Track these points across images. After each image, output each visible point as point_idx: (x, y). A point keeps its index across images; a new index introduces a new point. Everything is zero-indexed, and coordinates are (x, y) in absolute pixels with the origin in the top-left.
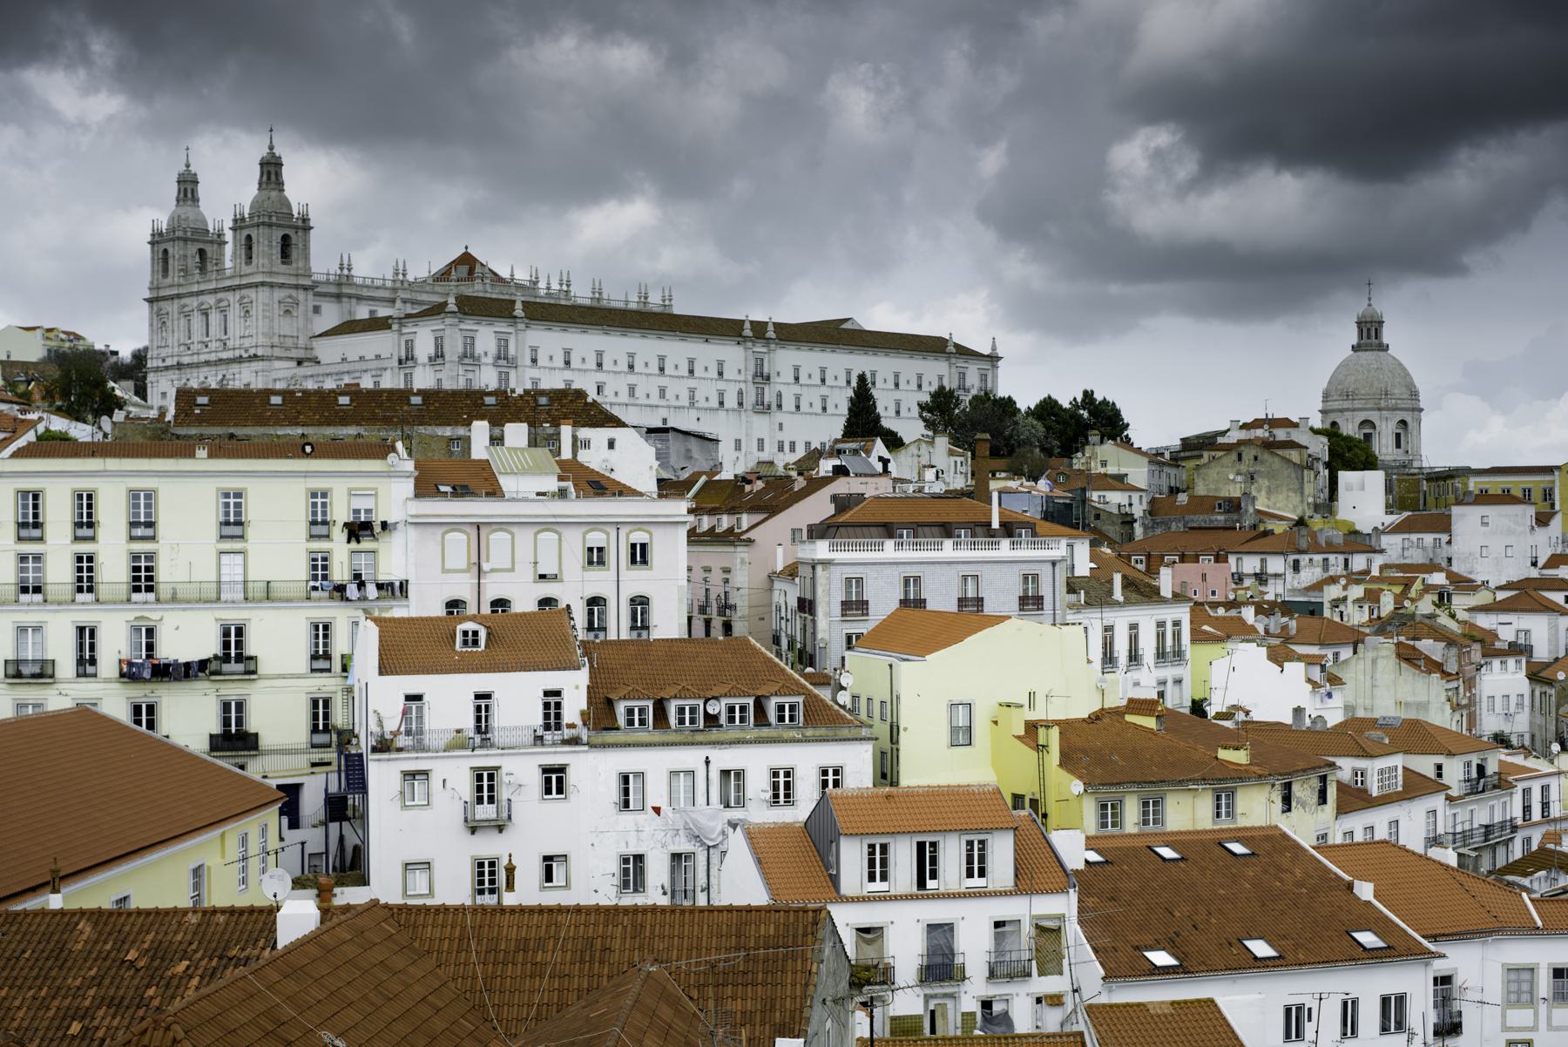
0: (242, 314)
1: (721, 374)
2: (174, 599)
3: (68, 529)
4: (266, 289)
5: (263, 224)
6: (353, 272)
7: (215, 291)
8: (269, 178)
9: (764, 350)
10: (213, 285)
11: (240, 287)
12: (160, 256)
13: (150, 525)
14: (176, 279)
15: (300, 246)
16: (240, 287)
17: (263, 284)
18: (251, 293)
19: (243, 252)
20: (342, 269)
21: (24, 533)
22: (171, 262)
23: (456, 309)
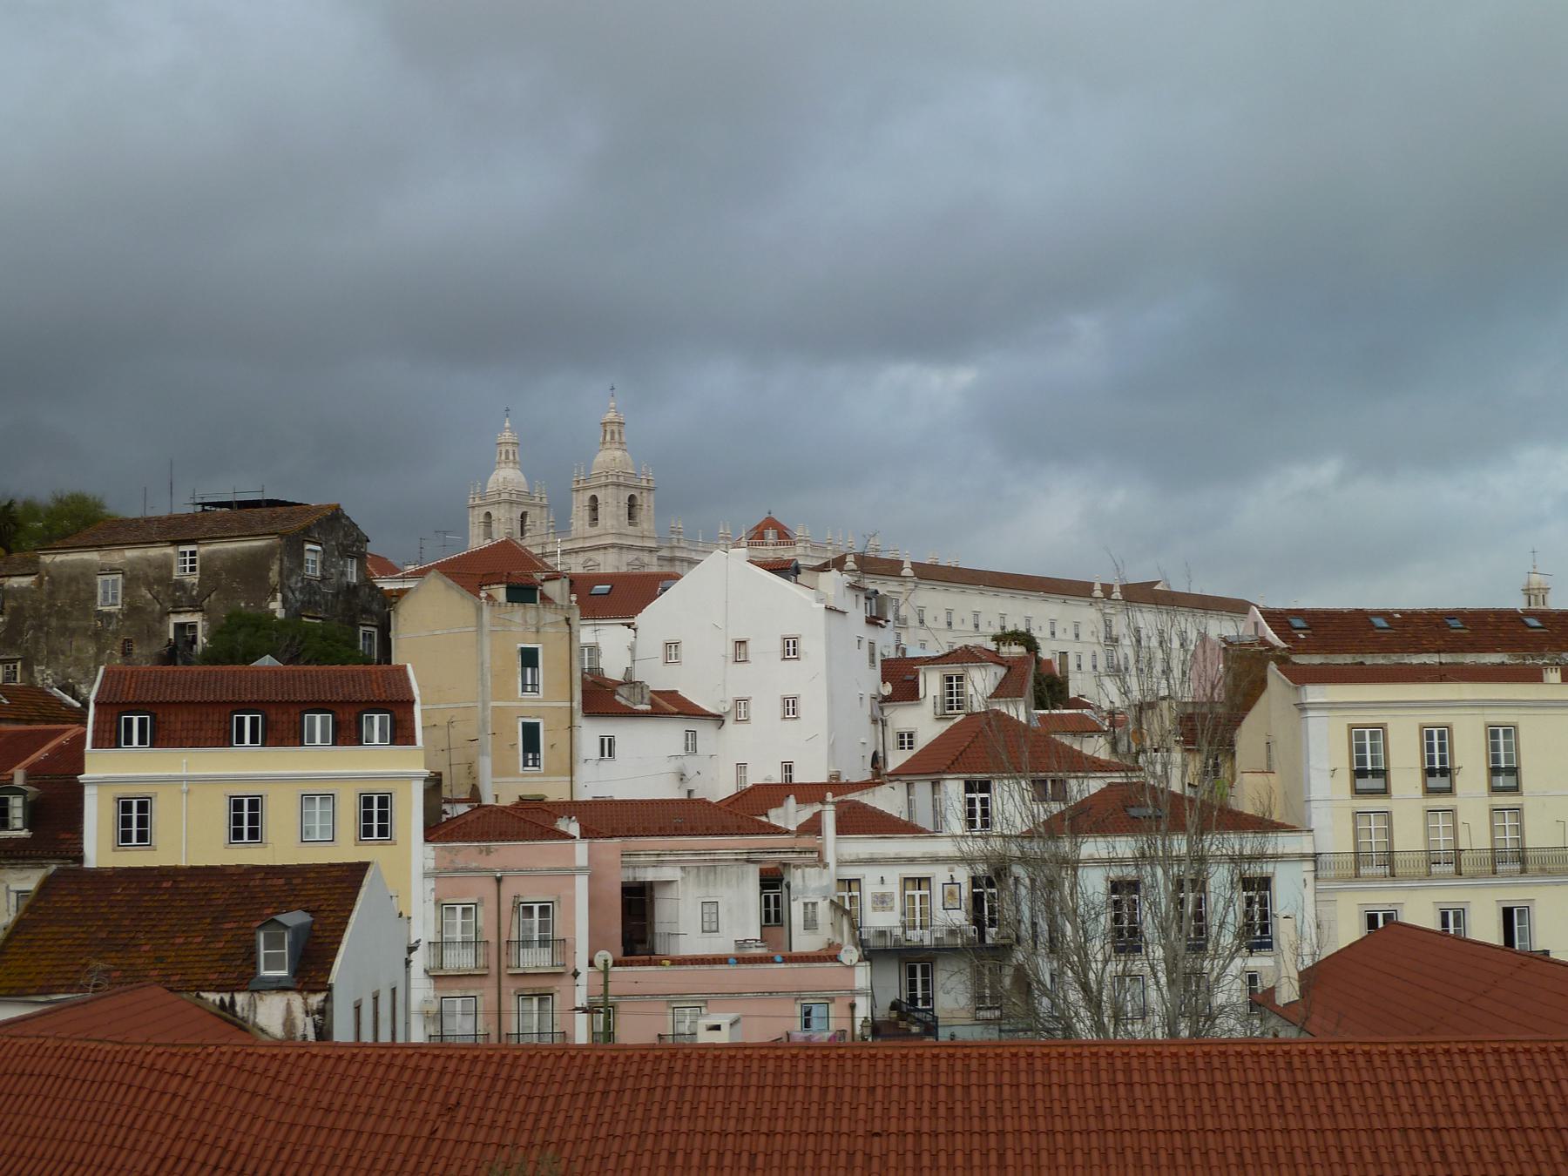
1: (1077, 636)
2: (1544, 871)
3: (1417, 777)
4: (615, 550)
5: (613, 484)
8: (612, 438)
9: (1113, 611)
13: (1513, 771)
15: (645, 506)
17: (613, 546)
19: (587, 513)
21: (1362, 784)
22: (495, 525)
23: (854, 567)
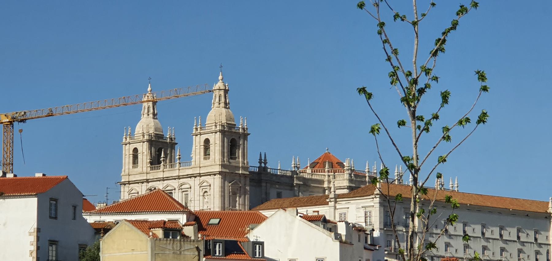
0: (202, 194)
6: (267, 165)
7: (179, 178)
10: (176, 173)
11: (200, 175)
12: (131, 152)
14: (145, 169)
16: (200, 175)
17: (220, 173)
18: (210, 179)
20: (260, 162)
